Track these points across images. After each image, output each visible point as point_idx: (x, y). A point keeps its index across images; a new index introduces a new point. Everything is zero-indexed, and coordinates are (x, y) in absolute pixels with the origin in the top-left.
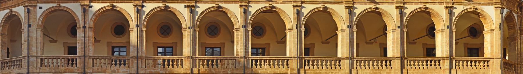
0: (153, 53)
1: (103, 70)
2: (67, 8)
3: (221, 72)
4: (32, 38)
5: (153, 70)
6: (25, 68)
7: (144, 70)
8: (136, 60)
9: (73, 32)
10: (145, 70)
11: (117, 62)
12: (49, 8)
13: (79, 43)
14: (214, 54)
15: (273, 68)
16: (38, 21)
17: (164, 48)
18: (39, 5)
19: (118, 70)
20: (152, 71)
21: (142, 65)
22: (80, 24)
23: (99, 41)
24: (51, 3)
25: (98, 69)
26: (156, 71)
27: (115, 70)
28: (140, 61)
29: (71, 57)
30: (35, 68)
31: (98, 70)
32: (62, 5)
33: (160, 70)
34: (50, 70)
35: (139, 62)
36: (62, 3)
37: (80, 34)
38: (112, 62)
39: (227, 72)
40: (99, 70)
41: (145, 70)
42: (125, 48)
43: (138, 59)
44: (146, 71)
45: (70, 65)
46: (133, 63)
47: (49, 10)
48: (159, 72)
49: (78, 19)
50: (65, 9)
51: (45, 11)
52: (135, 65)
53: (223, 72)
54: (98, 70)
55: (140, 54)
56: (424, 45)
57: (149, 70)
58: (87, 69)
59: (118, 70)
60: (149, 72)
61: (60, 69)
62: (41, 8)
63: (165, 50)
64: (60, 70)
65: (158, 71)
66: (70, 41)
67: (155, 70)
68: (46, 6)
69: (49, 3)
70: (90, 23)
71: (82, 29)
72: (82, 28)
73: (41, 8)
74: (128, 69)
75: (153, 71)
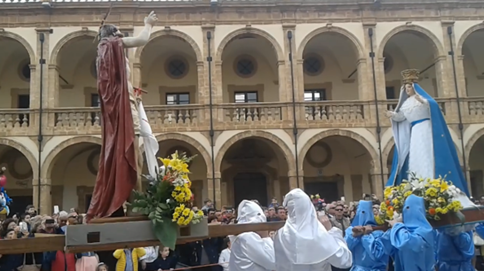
0: (84, 105)
5: (67, 129)
7: (52, 131)
8: (39, 114)
9: (26, 72)
10: (54, 130)
11: (23, 118)
14: (168, 103)
15: (258, 120)
17: (175, 95)
19: (9, 131)
20: (65, 131)
21: (48, 123)
22: (35, 59)
23: (71, 87)
26: (71, 131)
27: (5, 131)
28: (297, 108)
29: (24, 111)
32: (6, 29)
33: (79, 130)
35: (43, 118)
37: (35, 76)
38: (178, 114)
41: (54, 130)
42: (187, 96)
43: (43, 114)
44: (55, 131)
45: (256, 117)
46: (34, 120)
48: (76, 132)
49: (32, 51)
50: (178, 35)
55: (45, 106)
57: (60, 131)
59: (9, 131)
60: (61, 132)
63: (178, 98)
65: (74, 131)
66: (19, 84)
67: (70, 129)
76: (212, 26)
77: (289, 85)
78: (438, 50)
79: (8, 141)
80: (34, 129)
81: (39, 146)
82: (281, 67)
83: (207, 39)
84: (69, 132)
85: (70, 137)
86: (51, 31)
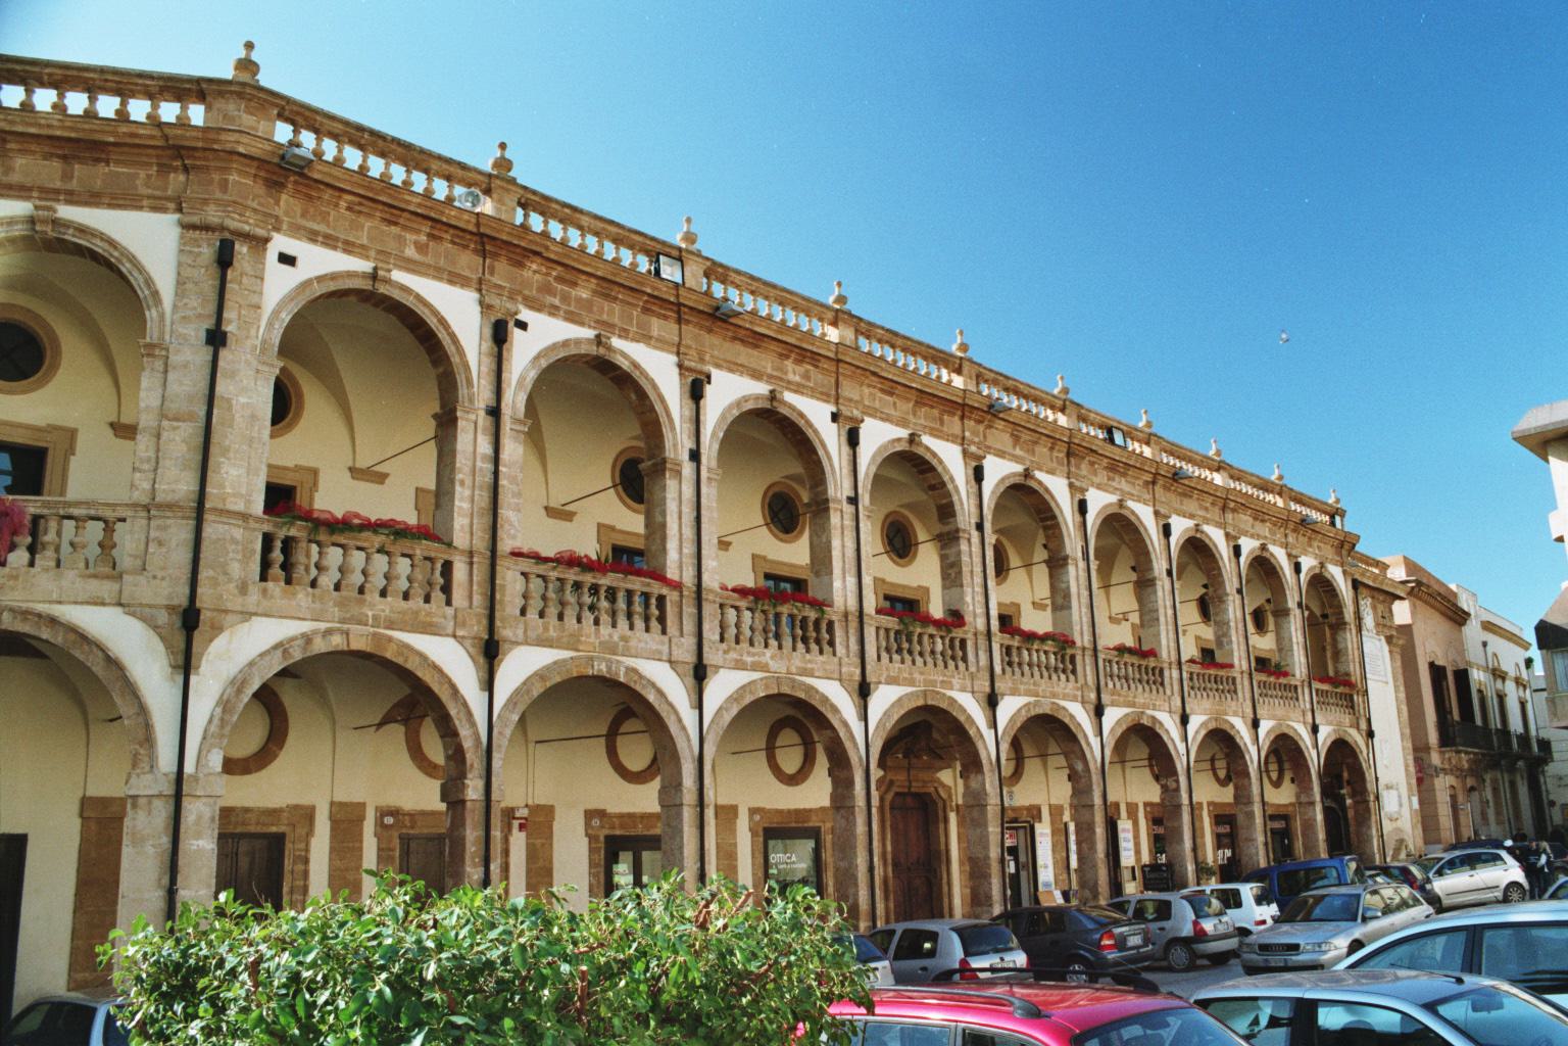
1: (566, 633)
2: (418, 297)
3: (936, 681)
4: (230, 408)
5: (749, 653)
6: (160, 574)
12: (333, 277)
13: (462, 483)
16: (270, 324)
18: (281, 243)
19: (624, 639)
24: (345, 251)
25: (546, 629)
26: (756, 658)
27: (616, 638)
30: (232, 586)
31: (546, 635)
34: (318, 606)
36: (400, 268)
39: (950, 682)
40: (552, 633)
47: (332, 286)
48: (767, 665)
51: (307, 284)
52: (689, 626)
53: (942, 682)
54: (546, 635)
56: (1197, 638)
58: (502, 621)
61: (372, 606)
62: (287, 260)
64: (370, 614)
65: (763, 659)
67: (754, 655)
68: (320, 262)
69: (335, 248)
70: (515, 400)
71: (483, 420)
72: (482, 413)
73: (287, 260)
74: (663, 643)
75: (749, 659)
76: (981, 453)
77: (1085, 610)
78: (1223, 582)
79: (623, 670)
80: (685, 651)
81: (695, 697)
82: (1071, 569)
83: (973, 482)
84: (753, 663)
85: (756, 675)
86: (709, 377)
